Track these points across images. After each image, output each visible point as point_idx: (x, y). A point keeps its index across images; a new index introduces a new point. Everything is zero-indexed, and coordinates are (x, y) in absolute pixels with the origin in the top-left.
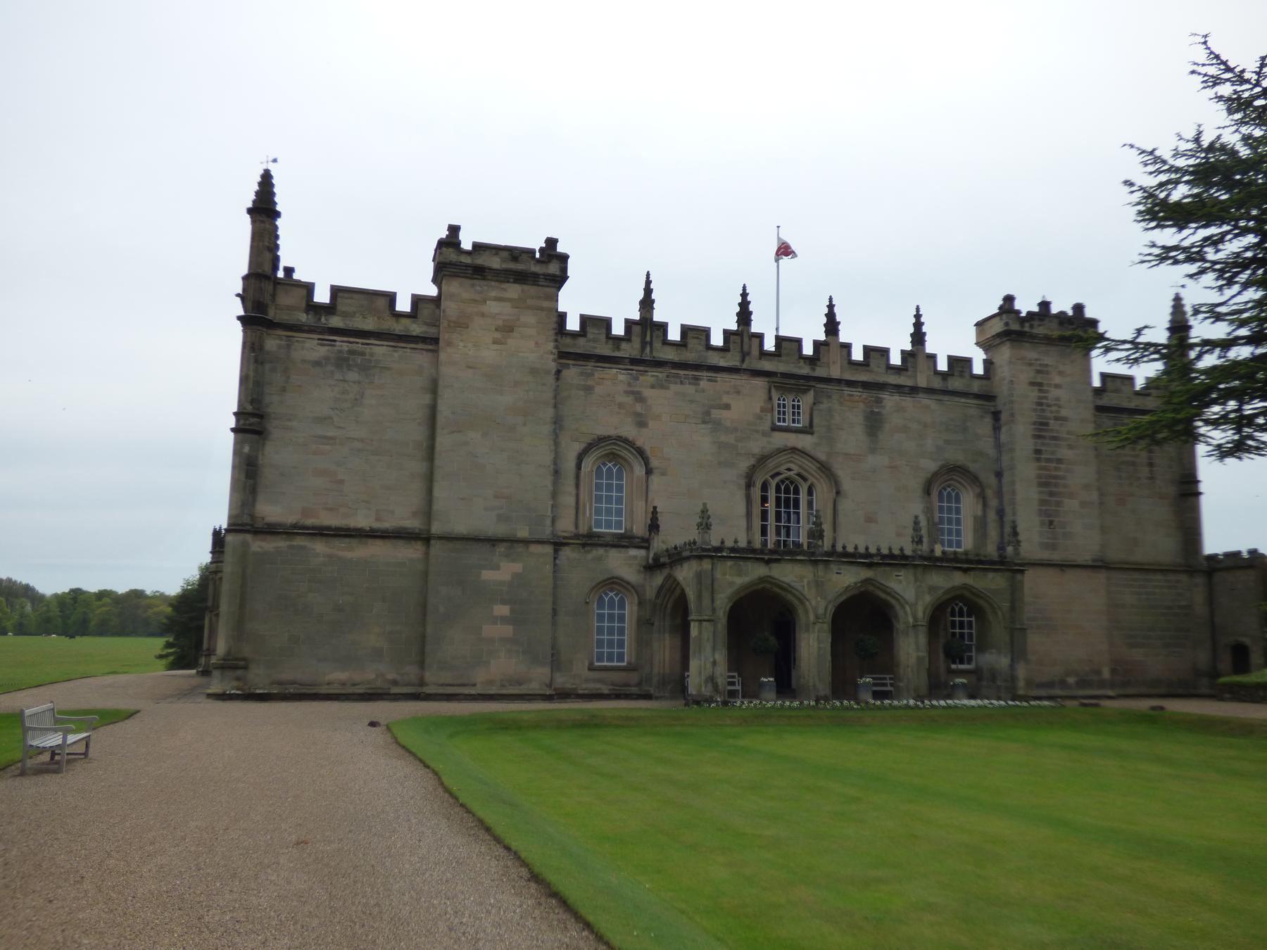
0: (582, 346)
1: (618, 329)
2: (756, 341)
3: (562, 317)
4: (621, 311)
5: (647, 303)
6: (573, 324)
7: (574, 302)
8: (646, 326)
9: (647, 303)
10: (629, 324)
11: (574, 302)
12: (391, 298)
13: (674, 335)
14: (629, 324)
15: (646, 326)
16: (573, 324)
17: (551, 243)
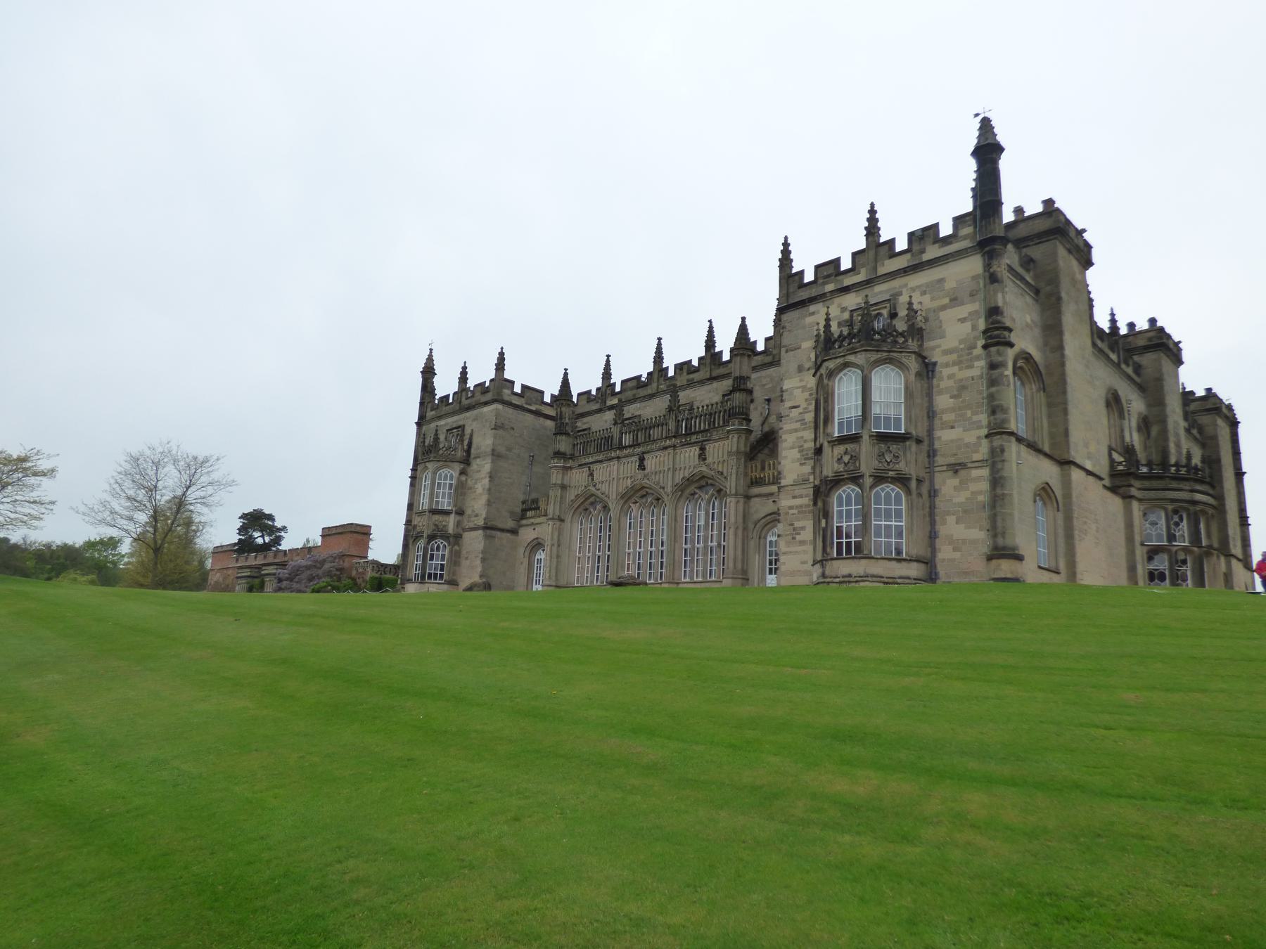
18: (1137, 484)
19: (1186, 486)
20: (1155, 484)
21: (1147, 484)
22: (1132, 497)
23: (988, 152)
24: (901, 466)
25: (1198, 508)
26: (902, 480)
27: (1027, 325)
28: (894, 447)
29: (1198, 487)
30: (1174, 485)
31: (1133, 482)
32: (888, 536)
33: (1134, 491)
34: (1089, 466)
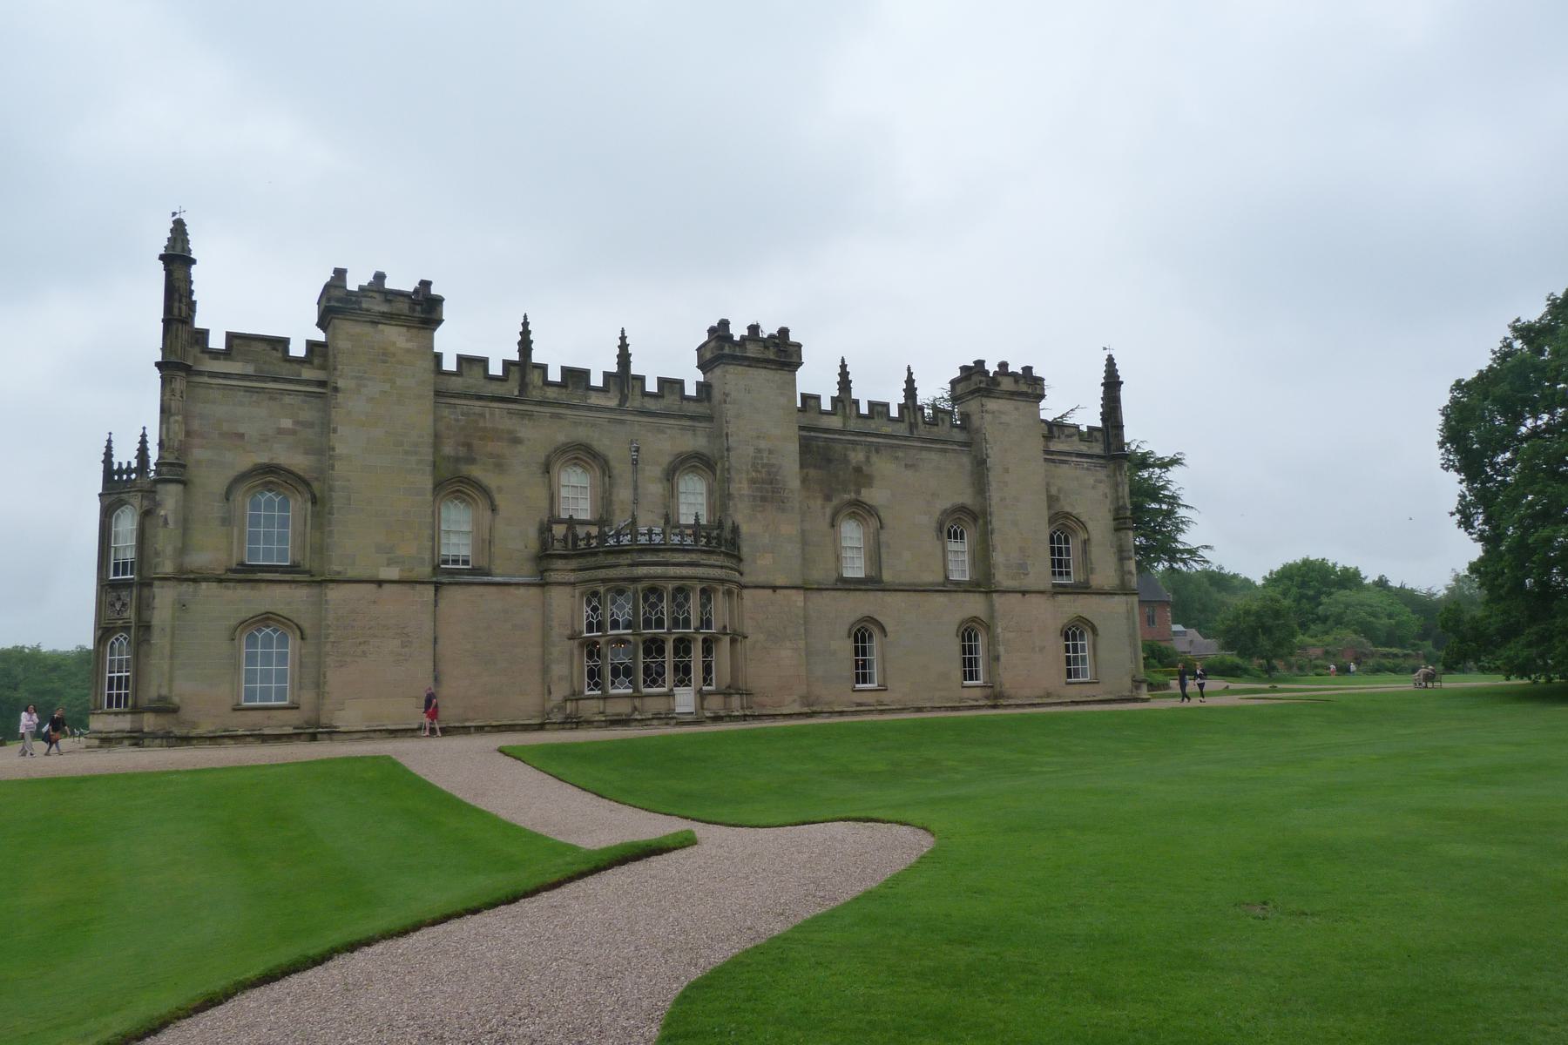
0: (457, 384)
1: (496, 369)
2: (537, 373)
3: (438, 358)
4: (499, 351)
5: (525, 345)
6: (449, 364)
7: (450, 342)
8: (523, 366)
9: (525, 345)
10: (507, 365)
11: (450, 342)
12: (284, 342)
13: (554, 375)
14: (507, 365)
15: (523, 366)
16: (449, 364)
17: (425, 284)
18: (574, 564)
19: (625, 559)
20: (592, 561)
21: (583, 562)
22: (548, 584)
23: (177, 260)
24: (126, 615)
25: (640, 586)
26: (126, 629)
27: (280, 431)
28: (124, 594)
29: (649, 558)
30: (611, 560)
31: (560, 564)
32: (119, 688)
33: (555, 577)
34: (393, 573)
